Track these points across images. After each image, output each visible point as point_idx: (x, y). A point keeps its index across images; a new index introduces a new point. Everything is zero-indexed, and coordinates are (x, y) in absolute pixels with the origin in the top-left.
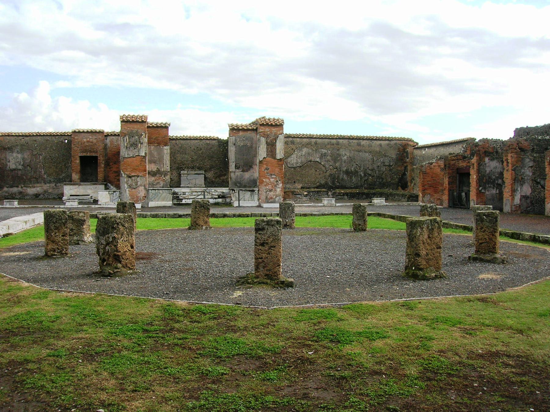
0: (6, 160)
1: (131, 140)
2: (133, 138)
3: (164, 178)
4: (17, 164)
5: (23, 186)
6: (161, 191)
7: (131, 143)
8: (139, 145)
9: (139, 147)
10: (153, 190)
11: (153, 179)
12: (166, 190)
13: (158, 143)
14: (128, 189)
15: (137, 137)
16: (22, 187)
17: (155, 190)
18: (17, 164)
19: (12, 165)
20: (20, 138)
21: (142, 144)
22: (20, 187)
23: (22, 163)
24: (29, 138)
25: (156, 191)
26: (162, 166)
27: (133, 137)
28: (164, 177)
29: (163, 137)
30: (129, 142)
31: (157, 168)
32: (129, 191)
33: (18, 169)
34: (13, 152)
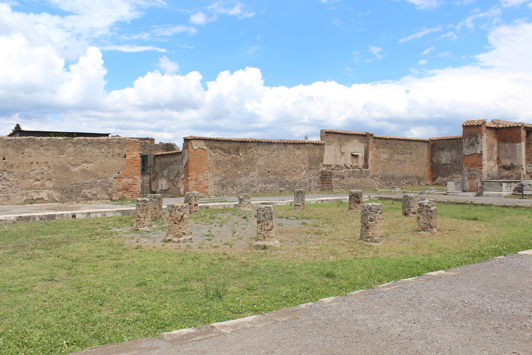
0: (440, 157)
1: (470, 141)
2: (472, 139)
3: (517, 172)
4: (447, 160)
5: (451, 176)
6: (493, 183)
7: (470, 143)
8: (476, 145)
9: (476, 146)
10: (487, 181)
11: (508, 172)
12: (497, 183)
13: (512, 142)
14: (468, 181)
15: (474, 138)
16: (450, 178)
17: (489, 182)
18: (447, 160)
19: (444, 160)
20: (449, 141)
21: (478, 143)
22: (449, 177)
23: (450, 159)
24: (455, 140)
25: (490, 182)
26: (515, 161)
27: (471, 138)
28: (517, 171)
29: (517, 135)
30: (469, 142)
31: (511, 163)
32: (469, 182)
33: (447, 164)
34: (444, 151)
